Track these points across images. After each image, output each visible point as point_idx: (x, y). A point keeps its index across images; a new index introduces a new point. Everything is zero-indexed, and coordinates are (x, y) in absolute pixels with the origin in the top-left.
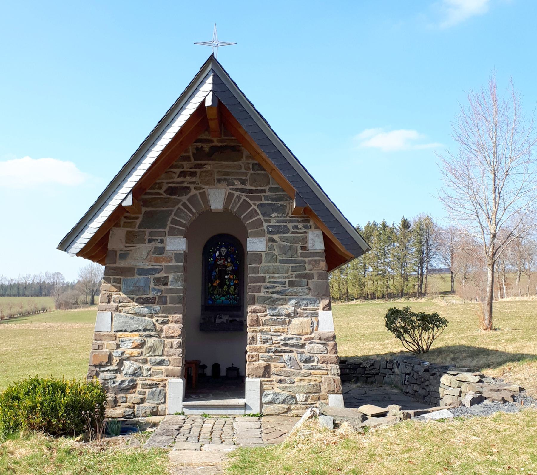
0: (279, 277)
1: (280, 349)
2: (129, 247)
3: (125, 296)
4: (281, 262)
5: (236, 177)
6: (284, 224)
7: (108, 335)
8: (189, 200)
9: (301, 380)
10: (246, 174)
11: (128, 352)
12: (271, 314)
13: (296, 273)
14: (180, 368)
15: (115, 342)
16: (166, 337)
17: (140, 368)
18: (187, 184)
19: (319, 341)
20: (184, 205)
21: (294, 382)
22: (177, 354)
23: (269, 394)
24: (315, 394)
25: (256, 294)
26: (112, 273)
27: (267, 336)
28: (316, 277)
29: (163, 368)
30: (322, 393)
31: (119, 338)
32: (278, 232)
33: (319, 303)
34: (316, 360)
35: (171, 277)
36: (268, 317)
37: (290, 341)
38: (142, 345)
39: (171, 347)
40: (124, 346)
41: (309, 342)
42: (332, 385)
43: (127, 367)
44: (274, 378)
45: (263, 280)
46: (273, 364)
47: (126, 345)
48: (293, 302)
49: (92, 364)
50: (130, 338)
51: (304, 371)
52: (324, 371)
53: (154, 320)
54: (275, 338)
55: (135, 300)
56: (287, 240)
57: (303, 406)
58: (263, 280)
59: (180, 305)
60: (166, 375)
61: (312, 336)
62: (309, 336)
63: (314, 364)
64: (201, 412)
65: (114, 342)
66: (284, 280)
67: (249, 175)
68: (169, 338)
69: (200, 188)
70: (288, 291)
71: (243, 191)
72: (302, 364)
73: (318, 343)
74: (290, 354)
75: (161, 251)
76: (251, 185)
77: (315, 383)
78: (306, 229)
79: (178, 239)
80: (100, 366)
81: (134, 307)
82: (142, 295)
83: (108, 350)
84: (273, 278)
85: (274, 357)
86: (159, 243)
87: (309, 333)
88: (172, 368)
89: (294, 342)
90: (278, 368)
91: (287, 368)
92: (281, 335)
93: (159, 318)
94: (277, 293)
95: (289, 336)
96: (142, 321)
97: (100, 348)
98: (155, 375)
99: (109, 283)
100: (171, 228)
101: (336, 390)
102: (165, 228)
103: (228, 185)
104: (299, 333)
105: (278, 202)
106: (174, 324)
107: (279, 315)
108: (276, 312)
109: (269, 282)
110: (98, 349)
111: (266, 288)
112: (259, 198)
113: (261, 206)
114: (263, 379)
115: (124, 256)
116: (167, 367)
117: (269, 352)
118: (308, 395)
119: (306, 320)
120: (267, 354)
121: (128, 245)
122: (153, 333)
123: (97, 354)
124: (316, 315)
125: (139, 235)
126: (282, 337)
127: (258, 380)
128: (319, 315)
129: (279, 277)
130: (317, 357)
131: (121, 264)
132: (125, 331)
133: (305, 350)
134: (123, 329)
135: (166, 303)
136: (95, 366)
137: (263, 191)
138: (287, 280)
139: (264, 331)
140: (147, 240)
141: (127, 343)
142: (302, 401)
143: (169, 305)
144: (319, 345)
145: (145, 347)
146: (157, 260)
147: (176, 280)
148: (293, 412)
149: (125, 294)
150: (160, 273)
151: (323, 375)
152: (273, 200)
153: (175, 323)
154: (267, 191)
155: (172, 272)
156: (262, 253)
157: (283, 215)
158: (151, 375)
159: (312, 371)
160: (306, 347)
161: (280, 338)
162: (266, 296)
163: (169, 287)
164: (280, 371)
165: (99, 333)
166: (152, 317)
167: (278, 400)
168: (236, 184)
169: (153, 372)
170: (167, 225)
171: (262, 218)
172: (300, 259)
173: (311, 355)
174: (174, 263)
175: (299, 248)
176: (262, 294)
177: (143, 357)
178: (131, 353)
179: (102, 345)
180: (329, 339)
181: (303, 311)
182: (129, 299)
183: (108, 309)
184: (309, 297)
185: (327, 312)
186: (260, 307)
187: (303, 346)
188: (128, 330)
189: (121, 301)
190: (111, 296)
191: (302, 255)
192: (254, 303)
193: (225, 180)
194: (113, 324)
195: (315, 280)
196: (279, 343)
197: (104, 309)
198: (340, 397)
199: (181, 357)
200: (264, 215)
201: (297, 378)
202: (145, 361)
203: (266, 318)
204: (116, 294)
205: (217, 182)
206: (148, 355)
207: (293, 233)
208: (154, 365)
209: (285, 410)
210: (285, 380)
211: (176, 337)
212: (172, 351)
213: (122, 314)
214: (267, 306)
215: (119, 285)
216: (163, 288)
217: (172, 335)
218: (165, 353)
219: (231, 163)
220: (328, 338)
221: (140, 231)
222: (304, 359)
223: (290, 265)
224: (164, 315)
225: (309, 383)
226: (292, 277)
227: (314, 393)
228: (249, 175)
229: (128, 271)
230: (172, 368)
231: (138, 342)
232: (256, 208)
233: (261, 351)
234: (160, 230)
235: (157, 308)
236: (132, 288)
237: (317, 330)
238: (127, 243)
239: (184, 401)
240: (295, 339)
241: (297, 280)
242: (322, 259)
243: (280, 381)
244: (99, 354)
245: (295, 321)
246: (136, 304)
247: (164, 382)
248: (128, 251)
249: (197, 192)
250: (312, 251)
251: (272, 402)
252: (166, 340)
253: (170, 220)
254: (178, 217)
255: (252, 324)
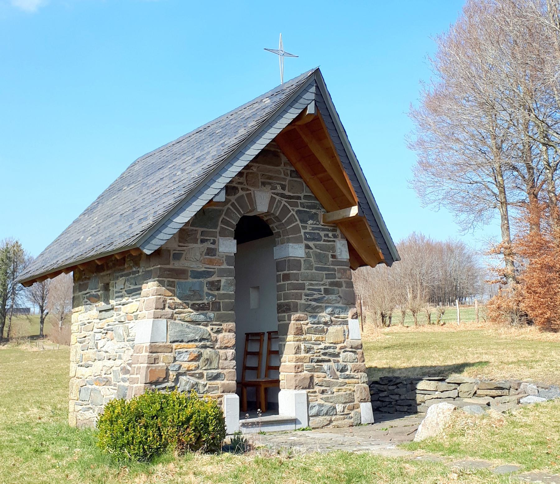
0: (317, 285)
1: (320, 358)
2: (182, 246)
3: (180, 301)
4: (317, 269)
5: (279, 182)
6: (318, 232)
7: (164, 346)
8: (237, 200)
9: (339, 389)
10: (284, 180)
11: (185, 365)
12: (312, 322)
13: (329, 280)
14: (235, 382)
15: (172, 355)
16: (221, 348)
17: (197, 384)
18: (236, 184)
19: (350, 350)
20: (233, 205)
21: (334, 392)
22: (232, 367)
23: (314, 406)
24: (351, 404)
25: (298, 301)
26: (168, 274)
27: (310, 345)
28: (344, 285)
29: (218, 382)
30: (355, 403)
31: (176, 349)
32: (314, 239)
33: (348, 311)
34: (349, 369)
35: (223, 280)
36: (310, 325)
37: (329, 350)
38: (198, 358)
39: (226, 359)
40: (180, 359)
41: (343, 350)
42: (363, 394)
43: (183, 383)
44: (317, 389)
45: (302, 287)
46: (316, 374)
47: (182, 357)
48: (329, 310)
49: (148, 381)
50: (186, 350)
51: (341, 380)
52: (356, 380)
53: (209, 328)
54: (315, 347)
55: (190, 306)
56: (321, 248)
57: (342, 416)
58: (302, 287)
59: (233, 312)
60: (222, 391)
61: (345, 344)
62: (342, 345)
63: (348, 373)
64: (257, 430)
65: (169, 354)
66: (320, 287)
67: (287, 181)
68: (223, 349)
69: (248, 190)
70: (325, 299)
71: (282, 195)
72: (338, 373)
73: (350, 352)
74: (329, 364)
75: (211, 252)
76: (289, 191)
77: (350, 392)
78: (334, 238)
79: (230, 240)
80: (156, 383)
81: (190, 313)
82: (197, 300)
83: (164, 364)
84: (311, 284)
85: (316, 367)
86: (211, 243)
87: (343, 342)
88: (228, 382)
89: (331, 351)
90: (321, 379)
91: (327, 377)
92: (320, 344)
93: (214, 327)
94: (315, 300)
95: (328, 345)
96: (198, 330)
97: (156, 362)
98: (211, 391)
99: (164, 286)
100: (222, 228)
101: (367, 398)
102: (216, 229)
103: (271, 189)
104: (334, 342)
105: (311, 210)
106: (227, 334)
107: (319, 323)
108: (316, 320)
109: (309, 289)
110: (154, 363)
111: (306, 295)
112: (296, 205)
113: (298, 212)
114: (308, 390)
115: (177, 257)
116: (223, 382)
117: (312, 362)
118: (345, 405)
119: (339, 328)
120: (310, 364)
121: (181, 244)
122: (208, 344)
123: (154, 368)
124: (346, 323)
125: (192, 234)
126: (322, 346)
127: (305, 392)
128: (349, 323)
129: (317, 285)
130: (350, 366)
131: (176, 265)
132: (182, 341)
133: (340, 359)
134: (180, 339)
135: (219, 310)
136: (151, 383)
137: (299, 198)
138: (322, 288)
139: (307, 339)
140: (199, 240)
141: (184, 355)
142: (340, 412)
143: (222, 312)
144: (351, 353)
145: (202, 359)
146: (211, 262)
147: (229, 284)
148: (334, 423)
149: (180, 299)
150: (213, 277)
151: (355, 383)
152: (308, 207)
153: (229, 332)
154: (302, 198)
155: (225, 275)
156: (301, 259)
157: (317, 223)
158: (207, 391)
159: (347, 380)
160: (340, 355)
161: (320, 347)
162: (306, 303)
163: (222, 292)
164: (322, 381)
165: (154, 344)
166: (206, 325)
167: (323, 412)
168: (278, 188)
169: (209, 387)
170: (217, 225)
171: (300, 225)
172: (332, 267)
173: (345, 364)
174: (225, 266)
175: (330, 256)
176: (303, 301)
177: (199, 371)
178: (188, 366)
179: (158, 358)
180: (358, 347)
181: (336, 319)
182: (184, 305)
183: (163, 317)
184: (340, 305)
185: (354, 320)
186: (303, 315)
187: (338, 355)
188: (184, 340)
189: (176, 307)
190: (166, 301)
191: (333, 263)
192: (296, 311)
193: (270, 184)
194: (168, 334)
195: (344, 288)
196: (319, 352)
197: (160, 316)
198: (369, 404)
199: (235, 370)
200: (302, 221)
201: (335, 388)
202: (201, 376)
203: (308, 327)
204: (170, 299)
205: (261, 185)
206: (204, 368)
207: (324, 241)
208: (209, 380)
209: (328, 422)
210: (326, 390)
211: (230, 347)
212: (226, 363)
213: (177, 321)
214: (308, 314)
215: (173, 289)
216: (216, 293)
217: (227, 345)
218: (220, 366)
219: (273, 167)
220: (357, 346)
221: (193, 230)
222: (341, 368)
223: (324, 273)
224: (219, 323)
225: (346, 393)
226: (326, 285)
227: (349, 403)
228: (287, 181)
229: (180, 273)
230: (228, 382)
231: (196, 354)
232: (294, 213)
233: (305, 361)
234: (211, 230)
235: (211, 314)
236: (188, 293)
237: (348, 338)
238: (180, 242)
239: (240, 419)
240: (332, 348)
241: (331, 288)
242: (347, 267)
243: (323, 392)
244: (155, 369)
245: (332, 329)
246: (192, 311)
247: (220, 399)
248: (182, 251)
249: (244, 193)
250: (340, 260)
251: (317, 415)
252: (219, 350)
253: (220, 220)
254: (228, 218)
255: (297, 333)
